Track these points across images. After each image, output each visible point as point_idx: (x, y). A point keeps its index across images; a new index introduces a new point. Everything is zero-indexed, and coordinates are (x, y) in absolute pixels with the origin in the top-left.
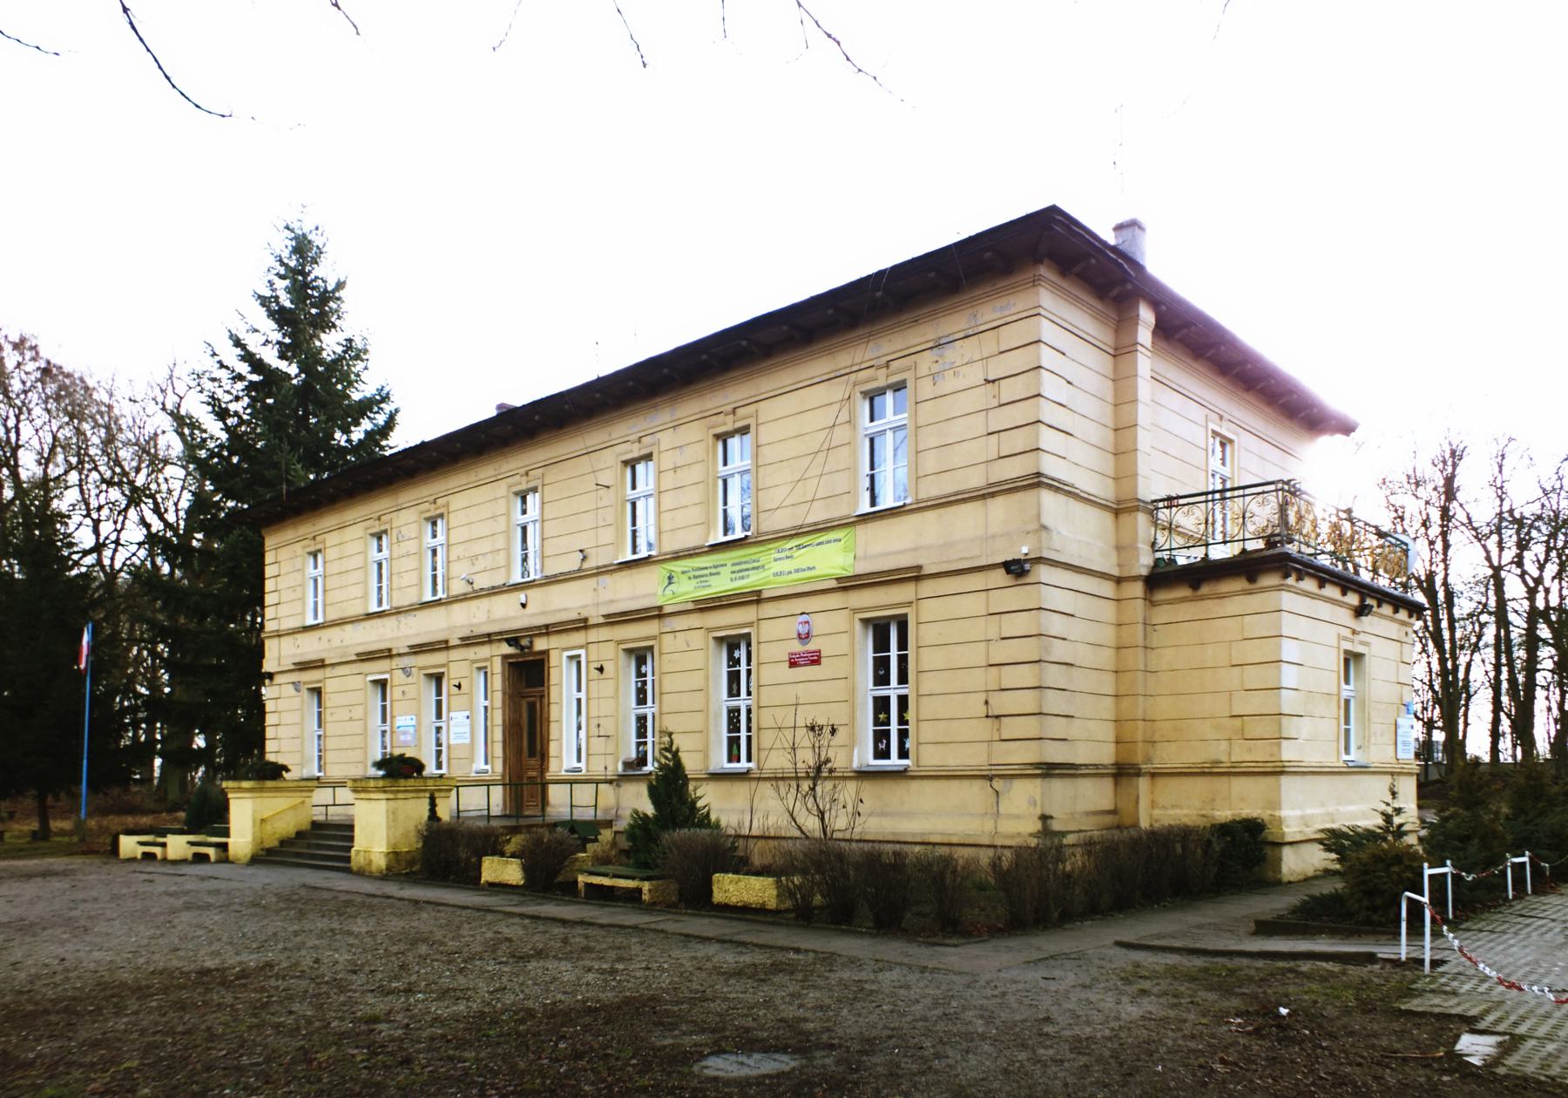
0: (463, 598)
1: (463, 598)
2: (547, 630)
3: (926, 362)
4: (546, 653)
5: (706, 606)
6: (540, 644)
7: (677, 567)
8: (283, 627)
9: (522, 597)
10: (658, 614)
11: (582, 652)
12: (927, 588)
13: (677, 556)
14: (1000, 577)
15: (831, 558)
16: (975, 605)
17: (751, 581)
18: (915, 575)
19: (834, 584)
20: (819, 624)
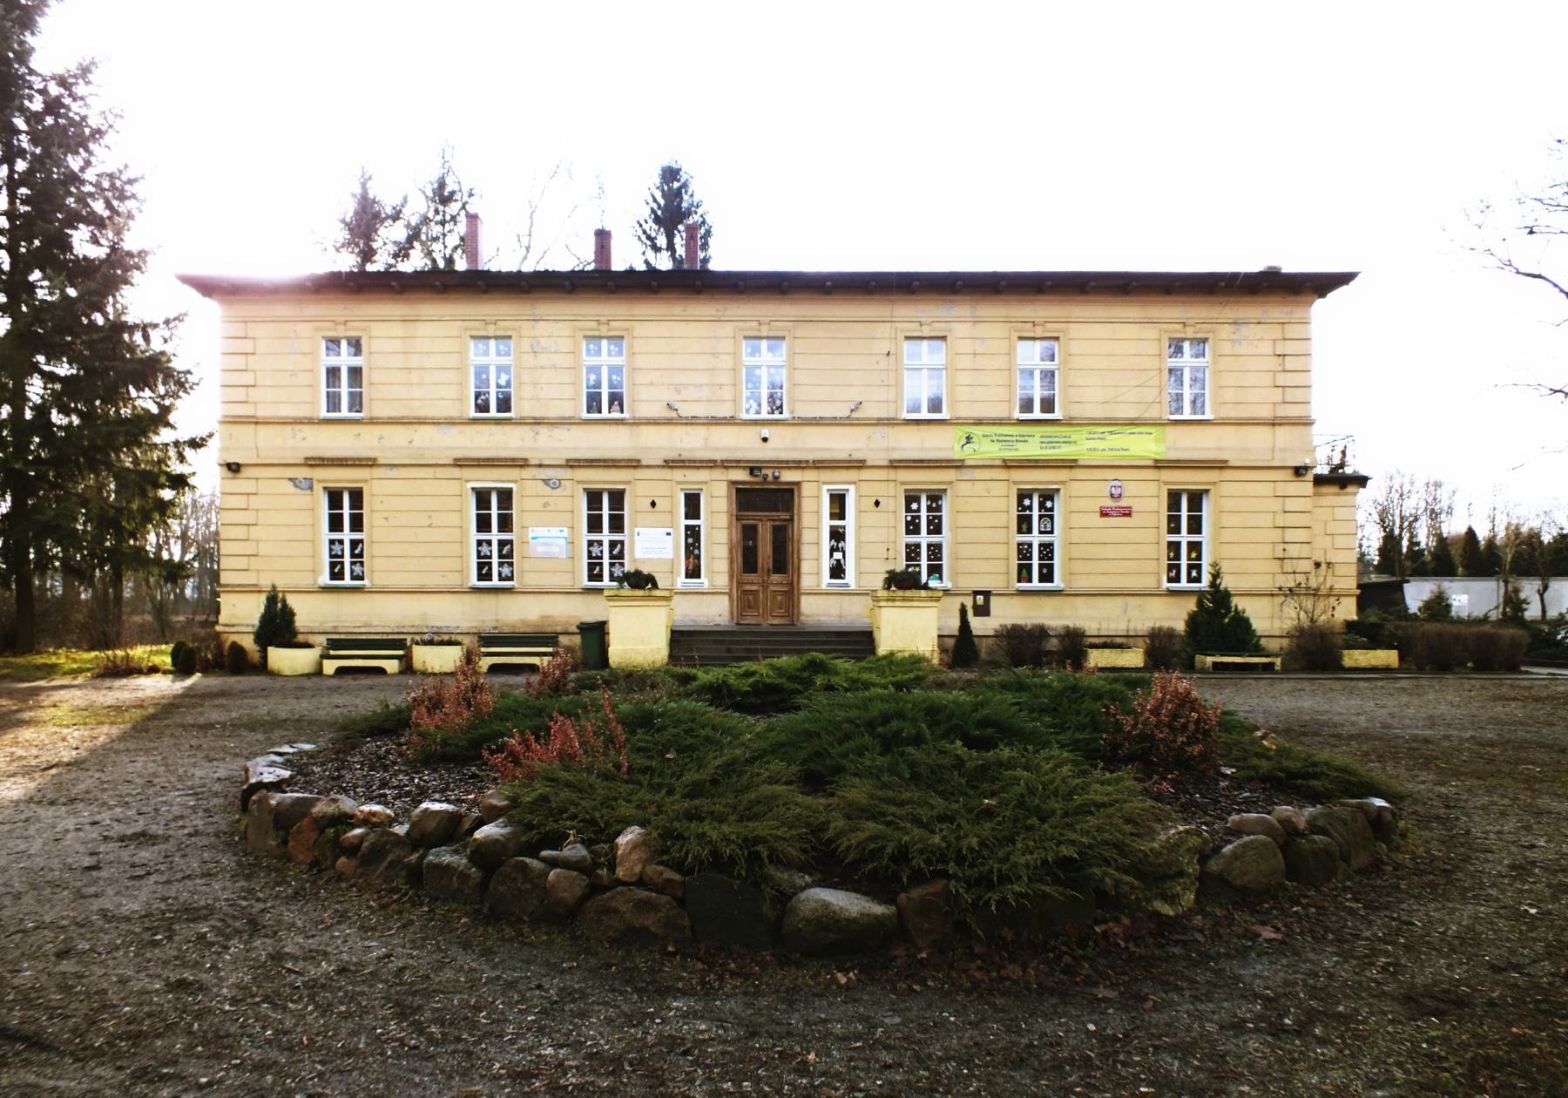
2: (799, 465)
3: (1226, 331)
4: (798, 484)
5: (1007, 465)
6: (788, 476)
7: (977, 431)
9: (765, 432)
10: (958, 465)
11: (852, 488)
12: (1227, 475)
13: (979, 422)
15: (1146, 445)
18: (1221, 465)
19: (1151, 463)
20: (1130, 489)
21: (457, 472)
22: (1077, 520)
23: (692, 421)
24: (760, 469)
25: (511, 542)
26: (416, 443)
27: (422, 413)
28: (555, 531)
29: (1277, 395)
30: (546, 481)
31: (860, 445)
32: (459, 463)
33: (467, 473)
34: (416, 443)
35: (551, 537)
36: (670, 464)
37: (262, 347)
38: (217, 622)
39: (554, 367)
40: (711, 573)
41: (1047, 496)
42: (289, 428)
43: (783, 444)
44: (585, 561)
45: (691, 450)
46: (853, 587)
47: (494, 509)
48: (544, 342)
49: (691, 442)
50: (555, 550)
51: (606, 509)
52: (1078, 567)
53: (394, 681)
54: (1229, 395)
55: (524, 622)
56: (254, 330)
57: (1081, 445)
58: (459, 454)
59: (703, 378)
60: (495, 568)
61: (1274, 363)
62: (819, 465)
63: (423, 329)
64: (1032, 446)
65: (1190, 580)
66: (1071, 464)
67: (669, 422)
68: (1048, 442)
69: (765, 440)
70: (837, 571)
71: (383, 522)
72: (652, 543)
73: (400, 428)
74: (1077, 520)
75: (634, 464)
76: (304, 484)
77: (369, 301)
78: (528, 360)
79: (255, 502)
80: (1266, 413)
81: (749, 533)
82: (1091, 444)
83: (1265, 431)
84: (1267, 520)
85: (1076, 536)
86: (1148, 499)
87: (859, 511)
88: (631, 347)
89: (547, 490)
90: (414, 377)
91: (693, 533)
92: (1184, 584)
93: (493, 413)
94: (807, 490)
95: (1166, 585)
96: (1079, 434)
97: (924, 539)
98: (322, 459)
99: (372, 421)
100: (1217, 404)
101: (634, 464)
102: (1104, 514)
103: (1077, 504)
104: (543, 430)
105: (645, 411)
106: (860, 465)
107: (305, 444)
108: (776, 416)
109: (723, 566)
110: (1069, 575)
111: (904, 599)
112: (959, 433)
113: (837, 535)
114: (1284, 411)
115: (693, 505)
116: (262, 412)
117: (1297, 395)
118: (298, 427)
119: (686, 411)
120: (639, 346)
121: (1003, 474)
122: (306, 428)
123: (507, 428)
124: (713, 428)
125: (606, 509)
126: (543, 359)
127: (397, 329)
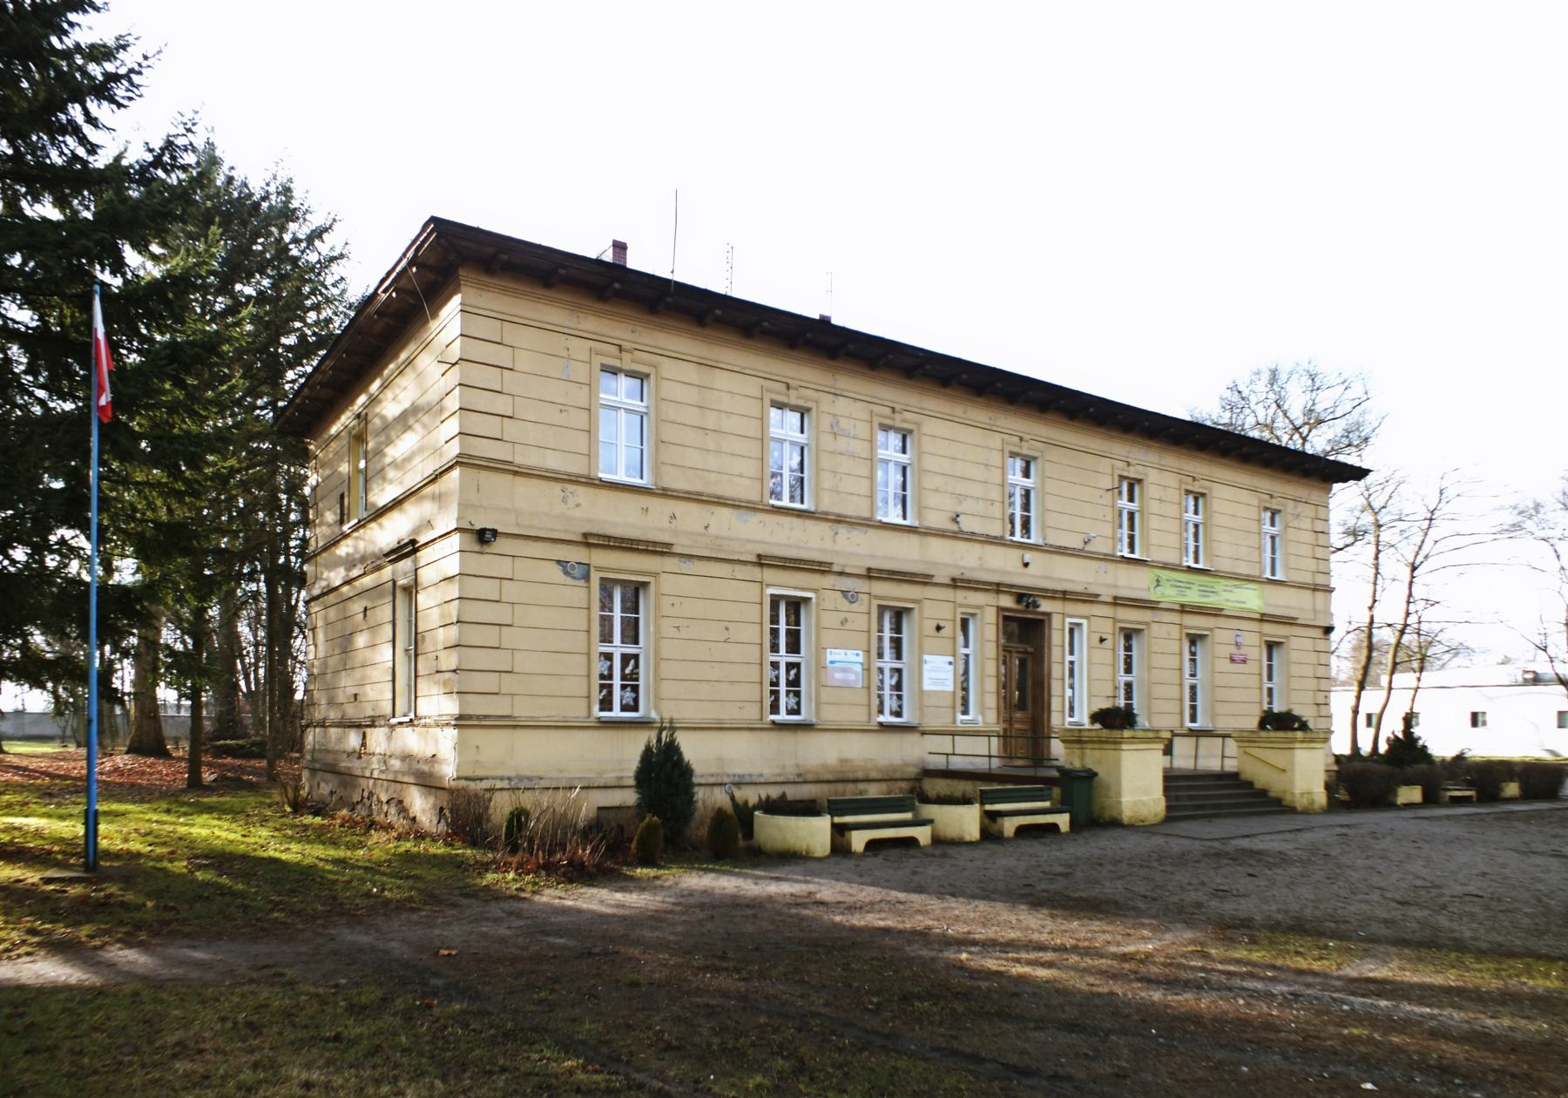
0: (941, 534)
1: (941, 534)
2: (1053, 595)
4: (1049, 615)
5: (1184, 609)
6: (1045, 606)
8: (519, 460)
9: (1028, 556)
11: (1084, 622)
14: (1318, 633)
16: (1308, 644)
17: (1211, 601)
21: (756, 573)
23: (971, 537)
32: (762, 561)
33: (769, 575)
36: (956, 584)
37: (524, 361)
40: (983, 709)
42: (558, 487)
43: (1043, 572)
45: (972, 569)
48: (844, 423)
50: (852, 677)
52: (1220, 708)
55: (824, 766)
59: (977, 491)
62: (1065, 596)
63: (722, 380)
66: (1216, 613)
68: (1205, 592)
69: (1026, 565)
73: (694, 508)
75: (924, 580)
76: (577, 572)
77: (662, 328)
78: (827, 441)
79: (510, 591)
80: (1308, 578)
87: (1090, 648)
90: (710, 441)
94: (1056, 622)
101: (924, 580)
104: (843, 530)
107: (577, 513)
109: (991, 701)
116: (523, 458)
118: (570, 488)
119: (967, 524)
122: (581, 490)
123: (809, 524)
126: (842, 444)
127: (691, 373)
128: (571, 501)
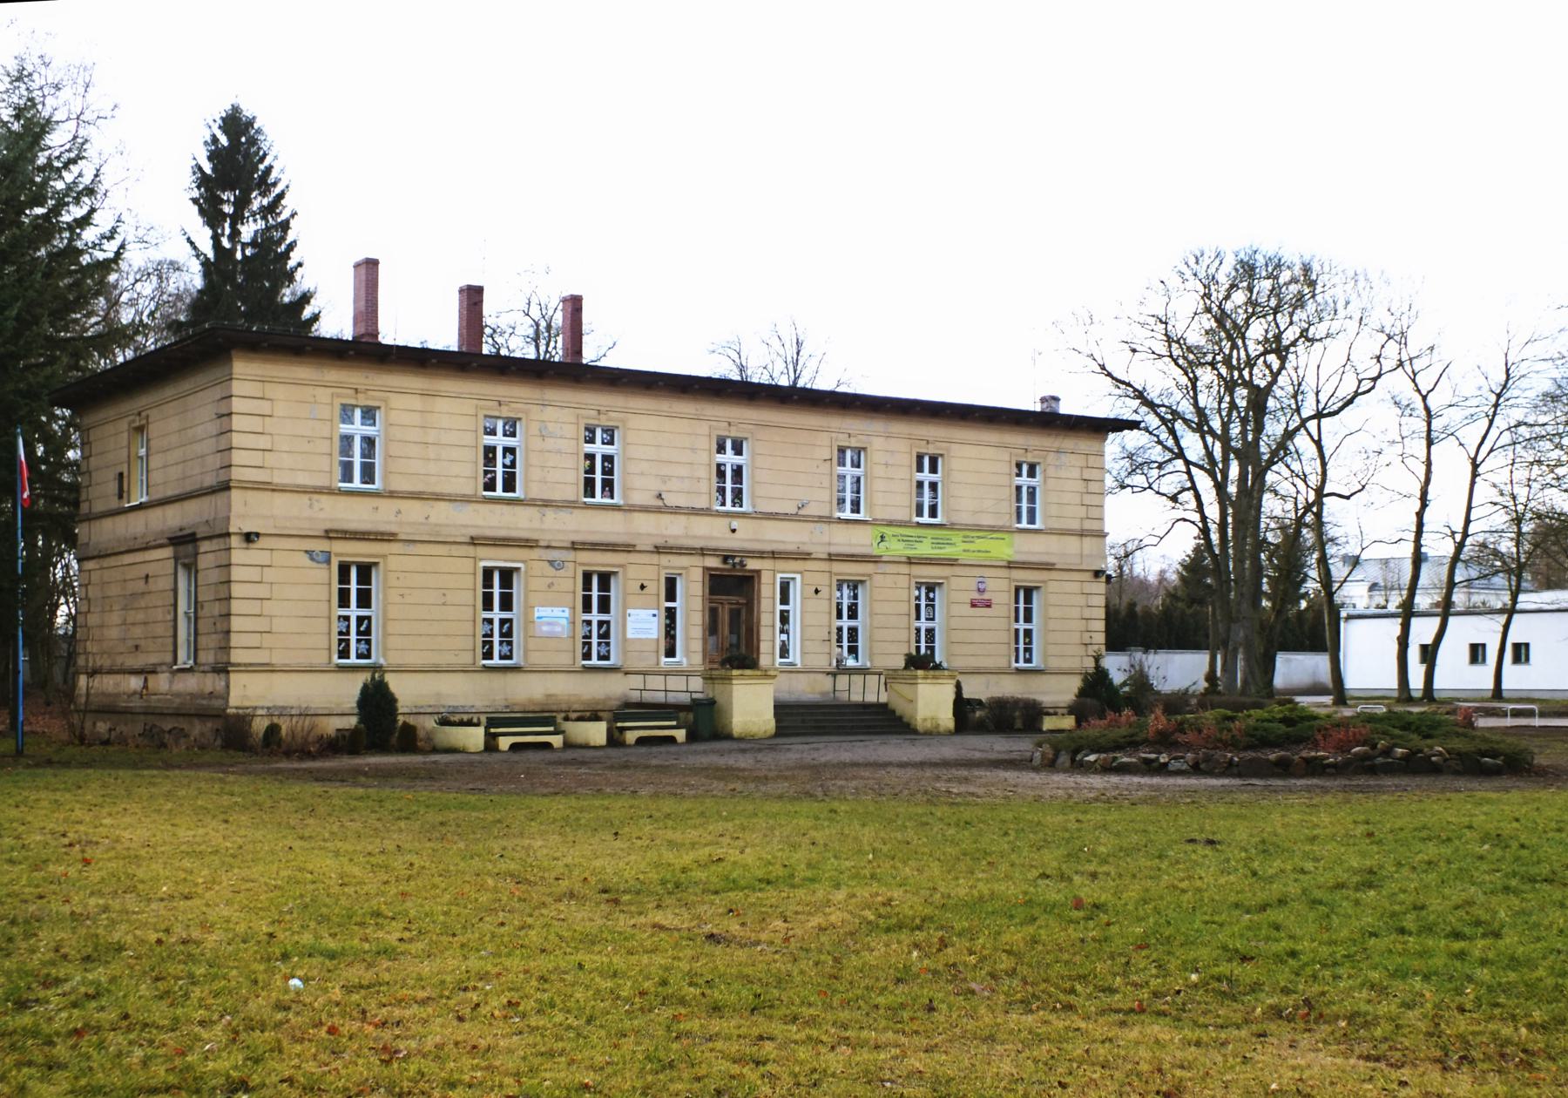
0: (645, 509)
1: (645, 509)
2: (761, 555)
3: (1051, 457)
4: (758, 572)
5: (910, 561)
6: (752, 564)
7: (888, 531)
8: (276, 480)
9: (735, 524)
10: (874, 560)
11: (798, 577)
12: (1054, 575)
13: (890, 523)
14: (1088, 576)
15: (1004, 549)
16: (1075, 587)
17: (948, 552)
18: (1048, 567)
20: (991, 585)
21: (471, 550)
22: (956, 610)
23: (676, 510)
24: (733, 557)
25: (369, 618)
26: (432, 520)
27: (438, 489)
28: (557, 612)
29: (1082, 512)
30: (551, 562)
31: (806, 539)
32: (474, 541)
33: (482, 551)
34: (432, 520)
35: (550, 616)
36: (658, 550)
37: (280, 409)
38: (227, 706)
39: (559, 452)
40: (687, 653)
41: (507, 576)
42: (305, 498)
43: (747, 535)
44: (516, 638)
45: (676, 537)
46: (798, 662)
47: (499, 586)
48: (551, 427)
49: (673, 529)
50: (558, 629)
51: (598, 589)
52: (957, 649)
53: (505, 757)
54: (1054, 510)
55: (531, 701)
56: (270, 391)
57: (956, 547)
58: (474, 532)
59: (683, 471)
60: (497, 646)
61: (1080, 486)
62: (774, 555)
63: (441, 404)
64: (357, 514)
65: (600, 658)
66: (951, 562)
67: (658, 510)
68: (938, 543)
69: (734, 531)
70: (784, 652)
71: (399, 600)
72: (640, 624)
73: (416, 504)
74: (956, 610)
75: (628, 548)
76: (320, 558)
77: (390, 371)
78: (536, 443)
79: (269, 575)
80: (1075, 525)
81: (713, 613)
82: (967, 546)
83: (1074, 541)
84: (1075, 613)
85: (954, 623)
86: (1000, 589)
87: (803, 598)
88: (624, 438)
89: (550, 571)
90: (432, 452)
91: (671, 614)
92: (353, 660)
93: (499, 492)
94: (765, 578)
95: (336, 660)
96: (957, 537)
97: (1022, 626)
98: (346, 532)
99: (392, 495)
100: (1046, 517)
101: (628, 548)
102: (973, 605)
103: (955, 596)
104: (550, 512)
105: (638, 498)
106: (805, 556)
107: (321, 515)
108: (737, 509)
109: (697, 646)
110: (1045, 656)
111: (935, 677)
112: (874, 532)
113: (784, 618)
114: (1088, 525)
115: (671, 585)
116: (279, 478)
117: (1094, 513)
118: (316, 497)
119: (671, 500)
120: (395, 416)
121: (904, 569)
122: (324, 498)
123: (518, 509)
124: (692, 518)
125: (598, 589)
126: (550, 444)
127: (416, 403)
128: (316, 506)
